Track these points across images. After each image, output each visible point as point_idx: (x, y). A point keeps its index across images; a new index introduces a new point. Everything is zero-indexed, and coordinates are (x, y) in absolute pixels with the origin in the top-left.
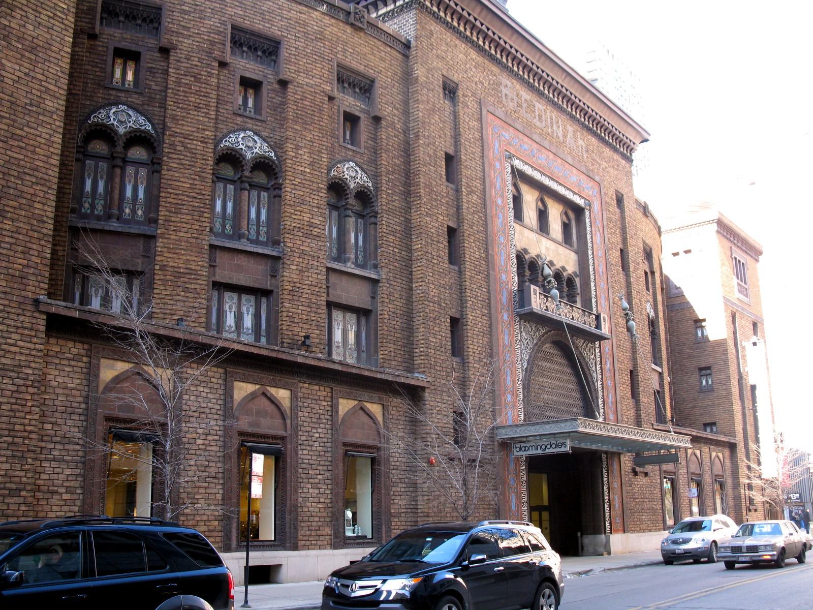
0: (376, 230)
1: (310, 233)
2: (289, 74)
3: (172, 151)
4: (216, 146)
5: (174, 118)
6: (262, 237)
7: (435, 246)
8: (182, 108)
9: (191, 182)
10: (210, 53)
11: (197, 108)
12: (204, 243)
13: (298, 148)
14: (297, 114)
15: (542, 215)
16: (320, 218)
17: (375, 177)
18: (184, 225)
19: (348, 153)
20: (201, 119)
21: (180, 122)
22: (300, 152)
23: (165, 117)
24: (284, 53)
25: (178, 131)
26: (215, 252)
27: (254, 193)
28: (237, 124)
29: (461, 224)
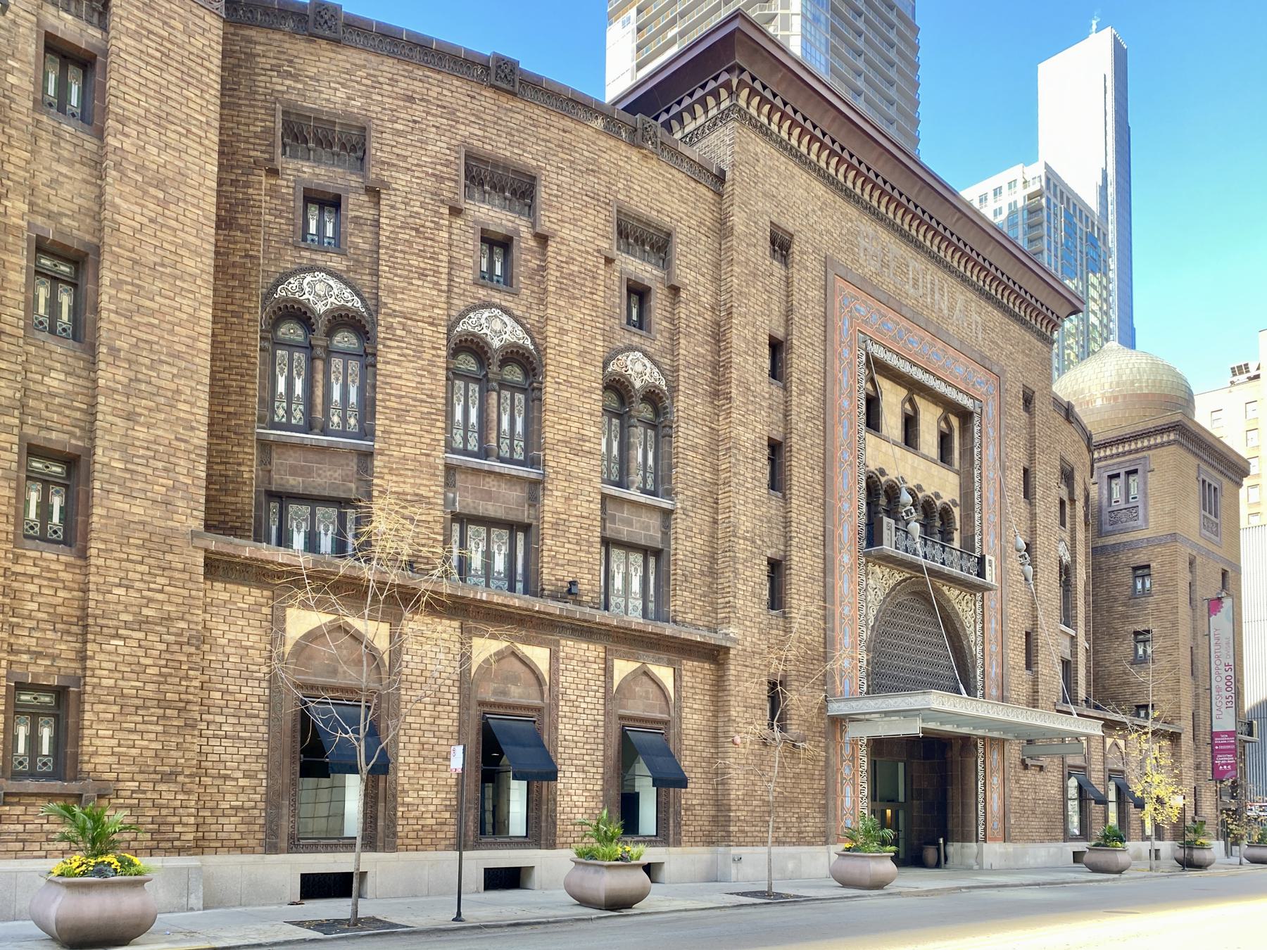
0: (671, 442)
1: (579, 448)
2: (548, 224)
3: (390, 336)
4: (450, 329)
5: (391, 291)
7: (750, 466)
8: (400, 276)
9: (418, 379)
10: (436, 194)
11: (422, 275)
12: (437, 461)
13: (562, 331)
14: (561, 283)
16: (593, 429)
18: (411, 438)
19: (633, 338)
20: (428, 291)
21: (399, 296)
22: (565, 338)
23: (378, 288)
24: (542, 194)
25: (397, 308)
26: (454, 475)
27: (506, 394)
28: (480, 299)
29: (788, 436)
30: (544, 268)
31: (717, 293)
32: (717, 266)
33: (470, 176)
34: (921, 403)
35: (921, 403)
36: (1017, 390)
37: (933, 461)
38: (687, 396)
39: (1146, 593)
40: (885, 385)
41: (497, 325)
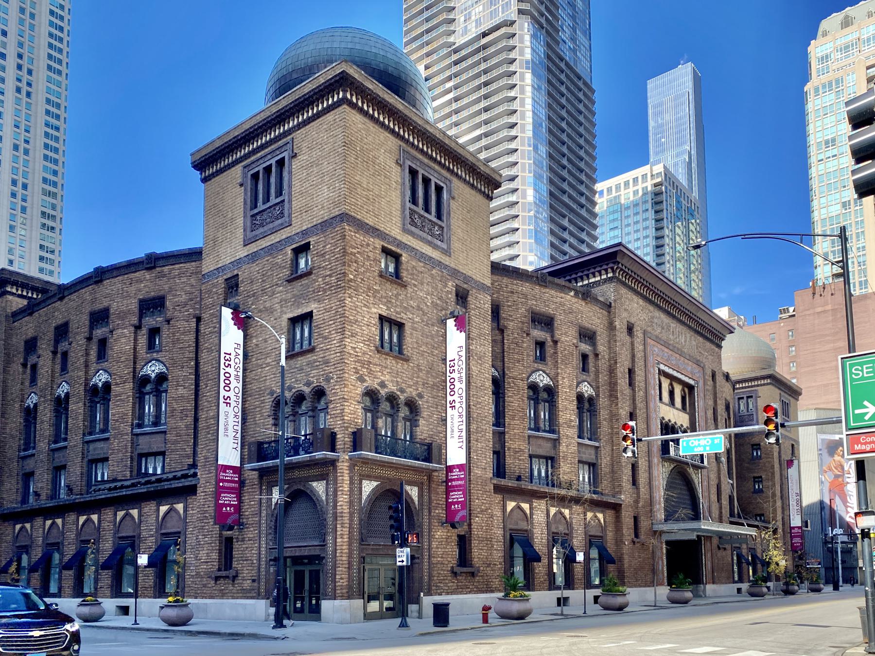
13: (563, 378)
17: (597, 389)
30: (556, 353)
31: (610, 353)
32: (609, 342)
33: (533, 321)
36: (709, 373)
37: (680, 410)
38: (602, 398)
39: (759, 458)
40: (663, 379)
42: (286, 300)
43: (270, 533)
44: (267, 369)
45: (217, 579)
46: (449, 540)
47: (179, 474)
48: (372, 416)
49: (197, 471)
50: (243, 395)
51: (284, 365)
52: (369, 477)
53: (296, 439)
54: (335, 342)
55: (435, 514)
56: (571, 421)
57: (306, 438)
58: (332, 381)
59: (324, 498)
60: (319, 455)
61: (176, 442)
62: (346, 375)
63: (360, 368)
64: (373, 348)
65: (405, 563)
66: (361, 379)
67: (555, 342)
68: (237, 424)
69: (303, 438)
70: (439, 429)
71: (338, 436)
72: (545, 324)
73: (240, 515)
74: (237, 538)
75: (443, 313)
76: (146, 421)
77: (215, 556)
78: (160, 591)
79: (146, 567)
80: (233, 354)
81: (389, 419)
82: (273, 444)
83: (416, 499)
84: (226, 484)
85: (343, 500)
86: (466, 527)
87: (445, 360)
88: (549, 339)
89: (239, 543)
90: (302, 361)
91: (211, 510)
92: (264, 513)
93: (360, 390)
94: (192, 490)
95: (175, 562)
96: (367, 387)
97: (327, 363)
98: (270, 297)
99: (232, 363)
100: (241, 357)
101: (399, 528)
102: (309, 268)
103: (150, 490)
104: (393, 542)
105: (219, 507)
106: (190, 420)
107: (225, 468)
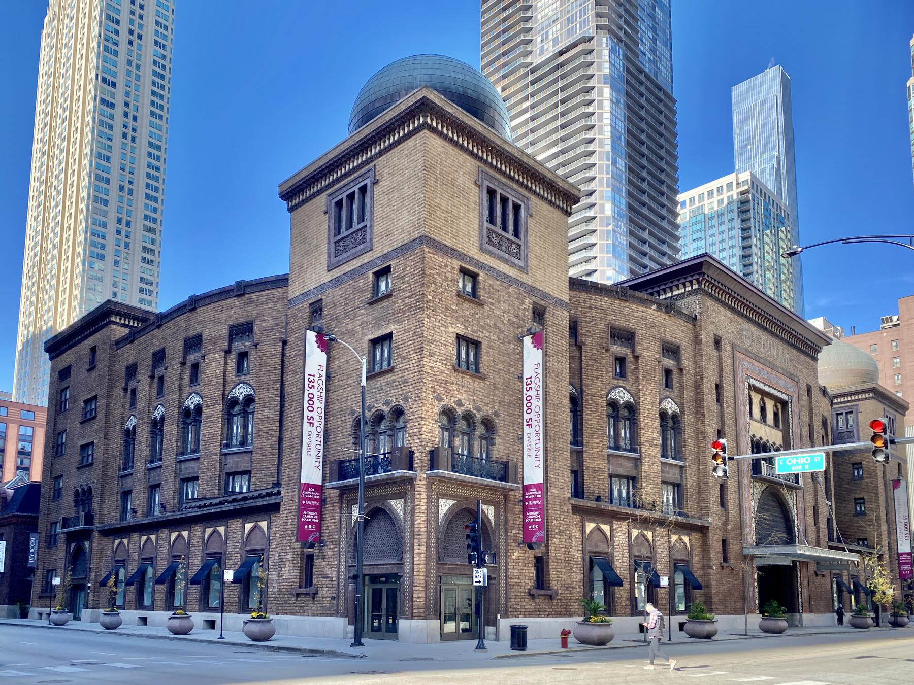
5: (587, 386)
6: (628, 447)
13: (645, 395)
15: (763, 410)
17: (681, 406)
30: (637, 369)
31: (696, 368)
32: (695, 356)
33: (613, 336)
34: (766, 400)
35: (766, 400)
36: (804, 387)
37: (772, 427)
39: (861, 478)
40: (753, 394)
41: (622, 395)
42: (367, 323)
43: (349, 551)
44: (348, 389)
45: (298, 595)
46: (526, 562)
47: (264, 492)
48: (449, 435)
49: (281, 489)
50: (325, 415)
51: (365, 385)
52: (446, 496)
53: (376, 457)
54: (414, 362)
55: (512, 535)
56: (654, 439)
57: (385, 457)
58: (410, 400)
59: (402, 517)
60: (397, 473)
61: (261, 462)
62: (424, 394)
63: (437, 387)
64: (450, 367)
65: (481, 584)
66: (438, 398)
67: (637, 358)
68: (319, 443)
69: (382, 457)
70: (515, 447)
71: (416, 455)
72: (625, 339)
73: (321, 533)
74: (317, 556)
75: (520, 330)
76: (234, 441)
77: (296, 572)
78: (244, 607)
79: (232, 582)
80: (317, 375)
81: (466, 438)
82: (353, 463)
83: (492, 519)
84: (308, 503)
85: (420, 518)
86: (543, 549)
87: (522, 377)
88: (629, 354)
89: (320, 560)
90: (382, 381)
91: (294, 528)
92: (344, 531)
93: (437, 409)
94: (276, 508)
95: (258, 578)
96: (445, 406)
97: (405, 382)
98: (351, 320)
99: (316, 384)
100: (324, 379)
101: (476, 549)
102: (389, 290)
103: (237, 507)
104: (470, 562)
105: (301, 524)
106: (275, 439)
107: (308, 486)
